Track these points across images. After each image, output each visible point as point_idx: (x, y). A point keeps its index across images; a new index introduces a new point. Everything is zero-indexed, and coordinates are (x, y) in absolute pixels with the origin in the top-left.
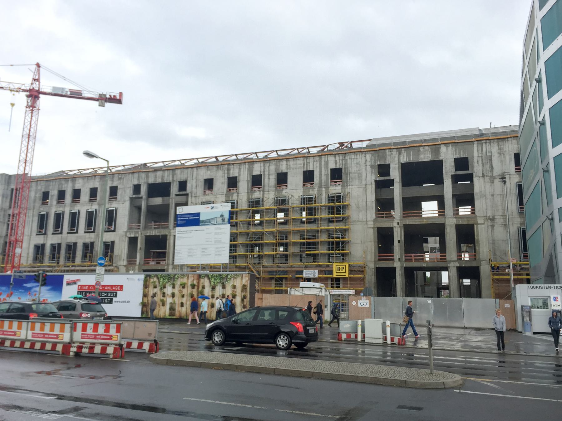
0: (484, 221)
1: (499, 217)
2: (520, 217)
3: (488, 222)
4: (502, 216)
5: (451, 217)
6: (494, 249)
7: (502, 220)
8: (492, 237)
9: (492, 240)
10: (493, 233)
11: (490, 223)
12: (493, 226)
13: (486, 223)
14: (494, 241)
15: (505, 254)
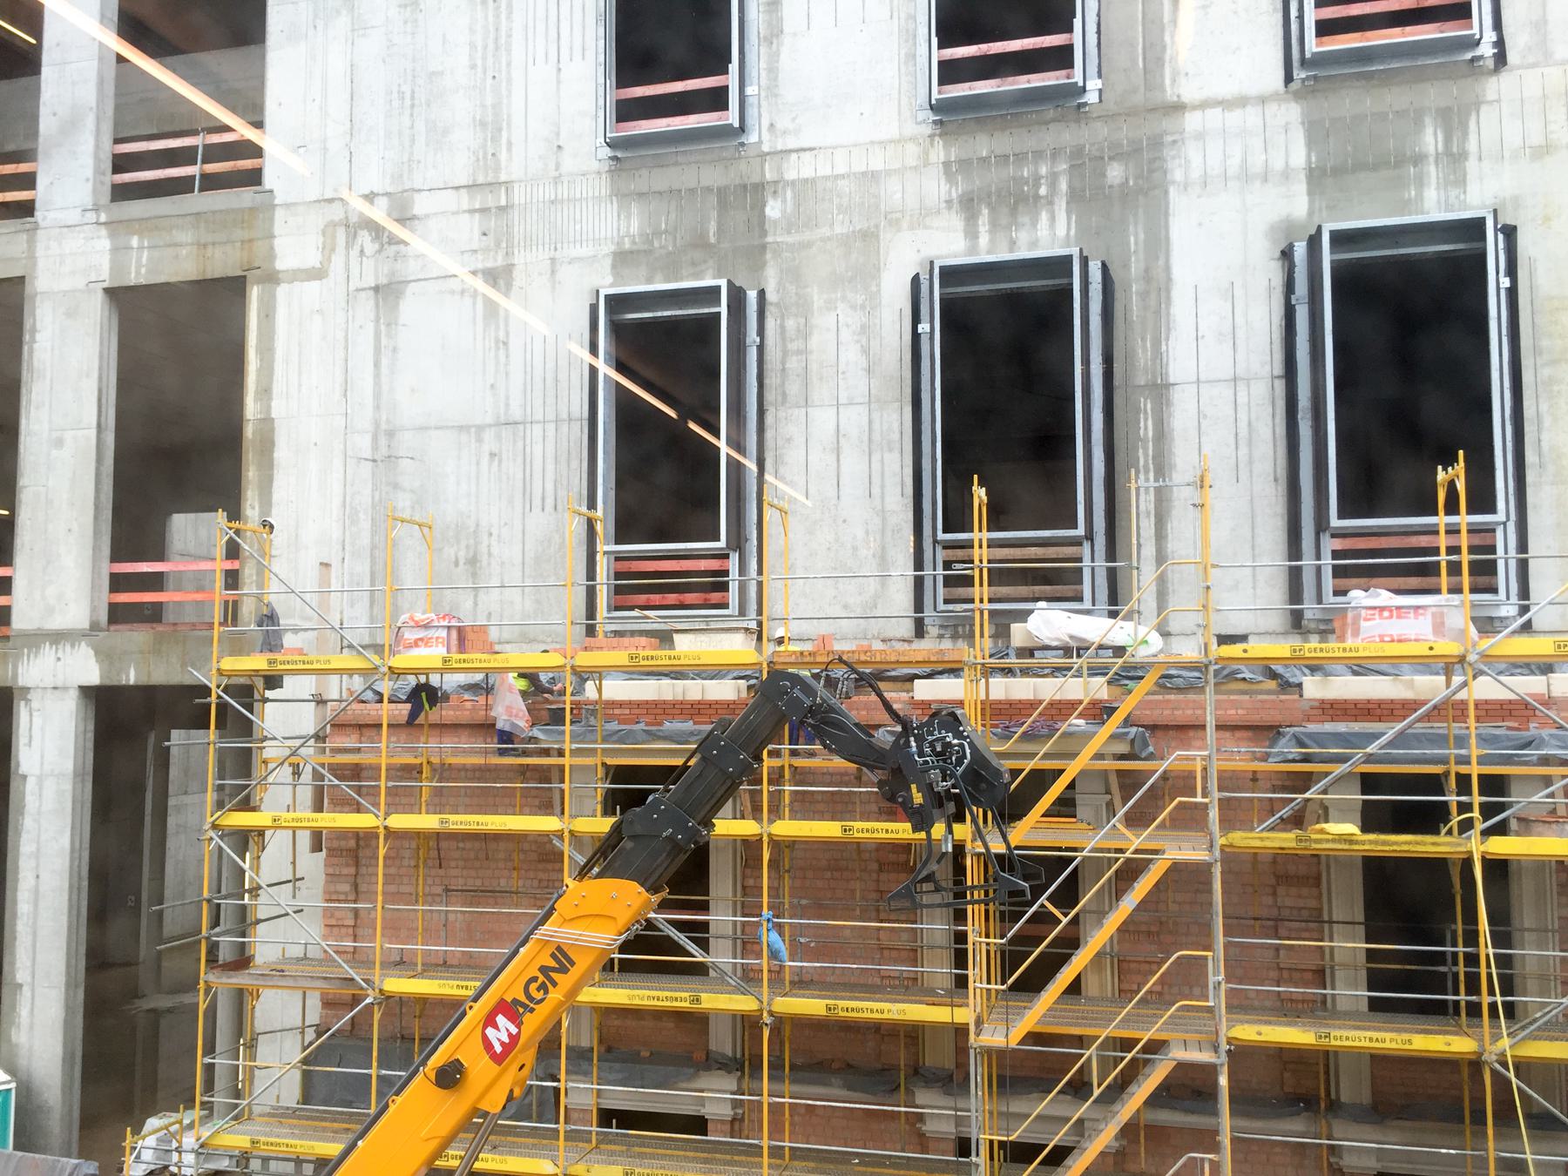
0: (328, 249)
1: (449, 200)
2: (622, 196)
3: (357, 248)
4: (472, 187)
5: (74, 217)
6: (387, 518)
7: (467, 230)
8: (377, 395)
9: (377, 424)
10: (384, 361)
11: (369, 264)
12: (387, 293)
13: (338, 261)
14: (391, 434)
15: (473, 561)
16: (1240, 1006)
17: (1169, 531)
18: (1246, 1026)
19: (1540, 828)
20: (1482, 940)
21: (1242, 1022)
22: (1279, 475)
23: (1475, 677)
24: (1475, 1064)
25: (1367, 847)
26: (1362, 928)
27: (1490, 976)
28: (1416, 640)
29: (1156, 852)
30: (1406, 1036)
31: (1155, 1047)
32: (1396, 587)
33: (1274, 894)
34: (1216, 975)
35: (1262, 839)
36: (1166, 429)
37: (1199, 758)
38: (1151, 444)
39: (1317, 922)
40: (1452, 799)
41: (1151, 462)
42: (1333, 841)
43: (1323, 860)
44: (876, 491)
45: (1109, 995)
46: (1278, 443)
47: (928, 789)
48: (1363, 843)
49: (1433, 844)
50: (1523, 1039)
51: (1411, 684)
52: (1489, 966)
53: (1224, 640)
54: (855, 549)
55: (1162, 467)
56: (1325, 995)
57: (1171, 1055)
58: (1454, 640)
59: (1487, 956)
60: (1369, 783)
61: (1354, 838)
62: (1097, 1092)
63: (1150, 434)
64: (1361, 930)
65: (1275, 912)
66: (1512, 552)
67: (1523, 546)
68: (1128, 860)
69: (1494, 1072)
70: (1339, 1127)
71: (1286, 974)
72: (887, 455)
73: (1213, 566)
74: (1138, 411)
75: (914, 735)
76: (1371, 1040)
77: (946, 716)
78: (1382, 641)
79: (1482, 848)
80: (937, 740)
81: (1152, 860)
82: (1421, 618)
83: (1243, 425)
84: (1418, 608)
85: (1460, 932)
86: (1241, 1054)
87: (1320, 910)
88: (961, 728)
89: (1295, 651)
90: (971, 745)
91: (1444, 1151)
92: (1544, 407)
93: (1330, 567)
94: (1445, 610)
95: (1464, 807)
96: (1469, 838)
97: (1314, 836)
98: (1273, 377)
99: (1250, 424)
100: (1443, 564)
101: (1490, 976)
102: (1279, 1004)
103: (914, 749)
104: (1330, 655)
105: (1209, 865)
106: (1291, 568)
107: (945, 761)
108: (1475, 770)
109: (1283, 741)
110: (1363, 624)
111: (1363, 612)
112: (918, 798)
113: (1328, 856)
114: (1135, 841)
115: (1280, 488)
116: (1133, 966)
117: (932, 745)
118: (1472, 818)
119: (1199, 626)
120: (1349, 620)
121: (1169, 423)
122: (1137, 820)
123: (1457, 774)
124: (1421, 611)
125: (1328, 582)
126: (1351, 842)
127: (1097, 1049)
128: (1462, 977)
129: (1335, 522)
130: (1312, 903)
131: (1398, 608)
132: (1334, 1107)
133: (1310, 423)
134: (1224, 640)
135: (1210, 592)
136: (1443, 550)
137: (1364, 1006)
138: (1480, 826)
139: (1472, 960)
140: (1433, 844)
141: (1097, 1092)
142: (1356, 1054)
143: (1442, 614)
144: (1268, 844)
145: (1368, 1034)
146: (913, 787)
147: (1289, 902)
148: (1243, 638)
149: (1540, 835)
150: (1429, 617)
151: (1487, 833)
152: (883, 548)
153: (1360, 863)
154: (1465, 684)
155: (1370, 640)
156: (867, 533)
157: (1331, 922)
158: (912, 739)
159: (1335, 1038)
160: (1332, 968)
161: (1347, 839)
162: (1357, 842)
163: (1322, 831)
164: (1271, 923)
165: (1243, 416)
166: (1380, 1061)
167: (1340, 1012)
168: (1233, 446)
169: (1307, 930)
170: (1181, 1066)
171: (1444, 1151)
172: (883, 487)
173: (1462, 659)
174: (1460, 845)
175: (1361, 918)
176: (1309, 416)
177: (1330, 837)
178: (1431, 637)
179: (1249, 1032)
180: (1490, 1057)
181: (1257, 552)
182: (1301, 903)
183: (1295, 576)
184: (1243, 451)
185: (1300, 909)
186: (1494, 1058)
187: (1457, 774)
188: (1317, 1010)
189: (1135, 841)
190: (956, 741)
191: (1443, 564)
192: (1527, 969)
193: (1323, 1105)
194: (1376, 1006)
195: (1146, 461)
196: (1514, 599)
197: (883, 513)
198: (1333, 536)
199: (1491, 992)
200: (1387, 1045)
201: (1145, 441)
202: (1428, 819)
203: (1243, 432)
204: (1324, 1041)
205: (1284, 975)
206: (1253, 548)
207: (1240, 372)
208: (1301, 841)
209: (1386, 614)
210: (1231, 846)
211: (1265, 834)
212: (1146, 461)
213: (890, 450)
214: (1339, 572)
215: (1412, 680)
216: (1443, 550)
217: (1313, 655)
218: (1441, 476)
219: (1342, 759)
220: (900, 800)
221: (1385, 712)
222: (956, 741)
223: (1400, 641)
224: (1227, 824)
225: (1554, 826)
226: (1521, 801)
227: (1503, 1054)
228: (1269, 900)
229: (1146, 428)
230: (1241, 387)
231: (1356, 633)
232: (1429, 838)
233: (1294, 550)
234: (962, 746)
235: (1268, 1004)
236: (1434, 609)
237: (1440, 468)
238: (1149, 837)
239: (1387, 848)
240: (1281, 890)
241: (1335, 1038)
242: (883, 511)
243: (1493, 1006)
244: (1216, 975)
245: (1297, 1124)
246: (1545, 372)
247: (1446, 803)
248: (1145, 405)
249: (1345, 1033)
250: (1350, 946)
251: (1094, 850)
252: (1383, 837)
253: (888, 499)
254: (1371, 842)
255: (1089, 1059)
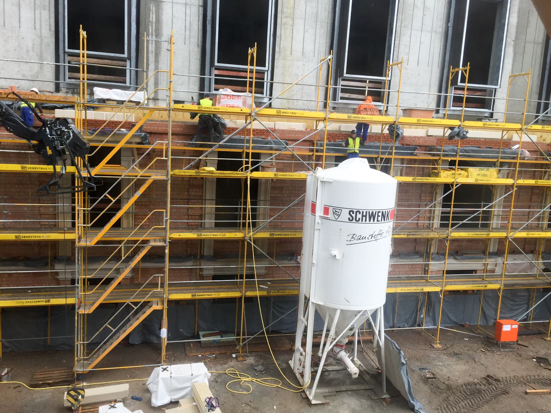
16: (175, 227)
17: (160, 60)
18: (175, 233)
19: (267, 169)
20: (248, 203)
21: (175, 232)
22: (199, 44)
23: (253, 121)
24: (243, 240)
25: (217, 175)
26: (215, 201)
27: (249, 214)
28: (237, 107)
29: (149, 177)
30: (224, 234)
31: (145, 242)
32: (234, 89)
33: (188, 191)
34: (167, 218)
35: (184, 172)
36: (160, 20)
37: (164, 144)
38: (154, 24)
39: (201, 199)
40: (244, 160)
41: (154, 32)
42: (207, 173)
43: (204, 180)
44: (38, 26)
45: (131, 226)
46: (200, 32)
47: (54, 148)
48: (216, 173)
49: (237, 174)
50: (257, 232)
51: (235, 123)
52: (249, 212)
53: (176, 102)
54: (28, 51)
55: (158, 34)
56: (202, 222)
57: (150, 244)
58: (249, 108)
59: (249, 208)
60: (220, 154)
61: (213, 172)
62: (123, 258)
63: (154, 20)
64: (214, 202)
65: (188, 197)
66: (269, 80)
67: (272, 79)
68: (138, 179)
69: (248, 242)
70: (202, 262)
71: (190, 217)
72: (42, 11)
73: (174, 74)
74: (150, 10)
75: (48, 127)
76: (214, 235)
77: (64, 122)
78: (227, 107)
79: (250, 175)
80: (58, 129)
81: (147, 179)
82: (239, 99)
83: (188, 22)
84: (239, 96)
85: (242, 202)
86: (174, 243)
87: (202, 196)
88: (69, 125)
89: (199, 108)
90: (73, 132)
91: (232, 266)
92: (282, 33)
93: (214, 79)
94: (247, 98)
95: (247, 163)
96: (247, 172)
97: (201, 171)
98: (199, 6)
99: (190, 23)
100: (248, 82)
101: (249, 214)
102: (187, 226)
103: (48, 132)
104: (211, 110)
105: (167, 181)
106: (201, 78)
107: (62, 138)
108: (251, 151)
109: (194, 140)
110: (222, 100)
111: (222, 96)
112: (50, 152)
113: (206, 178)
114: (141, 173)
115: (199, 49)
116: (140, 216)
117: (56, 131)
118: (248, 166)
119: (167, 96)
120: (217, 99)
121: (161, 17)
122: (142, 166)
123: (246, 152)
124: (239, 97)
125: (213, 86)
126: (212, 173)
127: (124, 244)
128: (242, 215)
129: (216, 64)
130: (200, 194)
131: (233, 95)
132: (202, 257)
133: (211, 26)
134: (176, 102)
135: (172, 83)
136: (248, 78)
137: (213, 225)
138: (250, 169)
139: (245, 210)
140: (237, 174)
141: (123, 258)
142: (210, 240)
143: (246, 99)
144: (187, 174)
145: (213, 234)
146: (48, 147)
147: (193, 194)
148: (182, 102)
149: (267, 171)
150: (242, 99)
151: (252, 171)
152: (41, 53)
153: (215, 180)
154: (250, 123)
155: (223, 106)
156: (34, 45)
157: (205, 200)
158: (47, 128)
159: (203, 235)
160: (205, 214)
161: (211, 172)
162: (214, 173)
163: (204, 170)
164: (186, 201)
165: (188, 19)
166: (217, 242)
167: (206, 228)
168: (184, 31)
169: (198, 202)
170: (153, 248)
171: (232, 266)
172: (41, 25)
173: (250, 115)
174: (244, 174)
175: (214, 198)
176: (210, 23)
177: (206, 172)
178: (242, 106)
179: (176, 235)
180: (247, 238)
181: (190, 71)
182: (197, 194)
183: (202, 81)
184: (187, 33)
185: (196, 196)
186: (248, 238)
187: (246, 152)
188: (200, 227)
189: (141, 173)
190: (66, 130)
191: (248, 82)
192: (261, 212)
193: (199, 257)
194: (217, 225)
195: (152, 31)
196: (268, 96)
197: (41, 37)
198: (216, 69)
199: (249, 219)
200: (218, 236)
201: (152, 23)
202: (236, 166)
203: (188, 26)
204: (200, 237)
205: (189, 217)
206: (189, 70)
207: (188, 2)
208: (197, 173)
209: (229, 97)
210: (174, 175)
211: (186, 171)
212: (152, 31)
213: (44, 9)
214: (217, 82)
215: (236, 121)
216: (248, 78)
217: (205, 110)
218: (250, 51)
219: (210, 146)
220: (42, 153)
221: (227, 131)
222: (66, 130)
223: (232, 107)
224: (173, 168)
225: (271, 168)
226: (264, 161)
227: (250, 237)
228: (186, 193)
229: (153, 18)
230: (188, 7)
231: (219, 103)
232: (235, 172)
233: (203, 72)
234: (69, 132)
235: (184, 226)
236: (243, 97)
237: (250, 48)
238: (145, 172)
239: (223, 175)
240: (190, 190)
241: (203, 235)
242: (41, 36)
243: (249, 223)
244: (167, 218)
245: (190, 263)
246: (284, 20)
247: (242, 161)
248: (153, 8)
249: (206, 234)
250: (210, 207)
251: (125, 176)
252: (222, 172)
253: (43, 31)
254: (218, 173)
255: (121, 247)
